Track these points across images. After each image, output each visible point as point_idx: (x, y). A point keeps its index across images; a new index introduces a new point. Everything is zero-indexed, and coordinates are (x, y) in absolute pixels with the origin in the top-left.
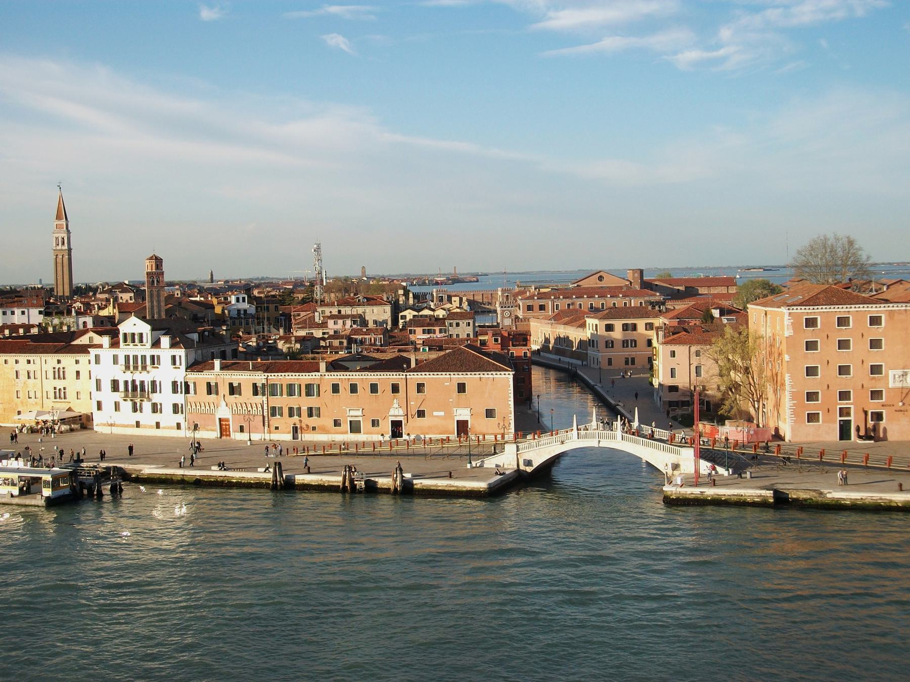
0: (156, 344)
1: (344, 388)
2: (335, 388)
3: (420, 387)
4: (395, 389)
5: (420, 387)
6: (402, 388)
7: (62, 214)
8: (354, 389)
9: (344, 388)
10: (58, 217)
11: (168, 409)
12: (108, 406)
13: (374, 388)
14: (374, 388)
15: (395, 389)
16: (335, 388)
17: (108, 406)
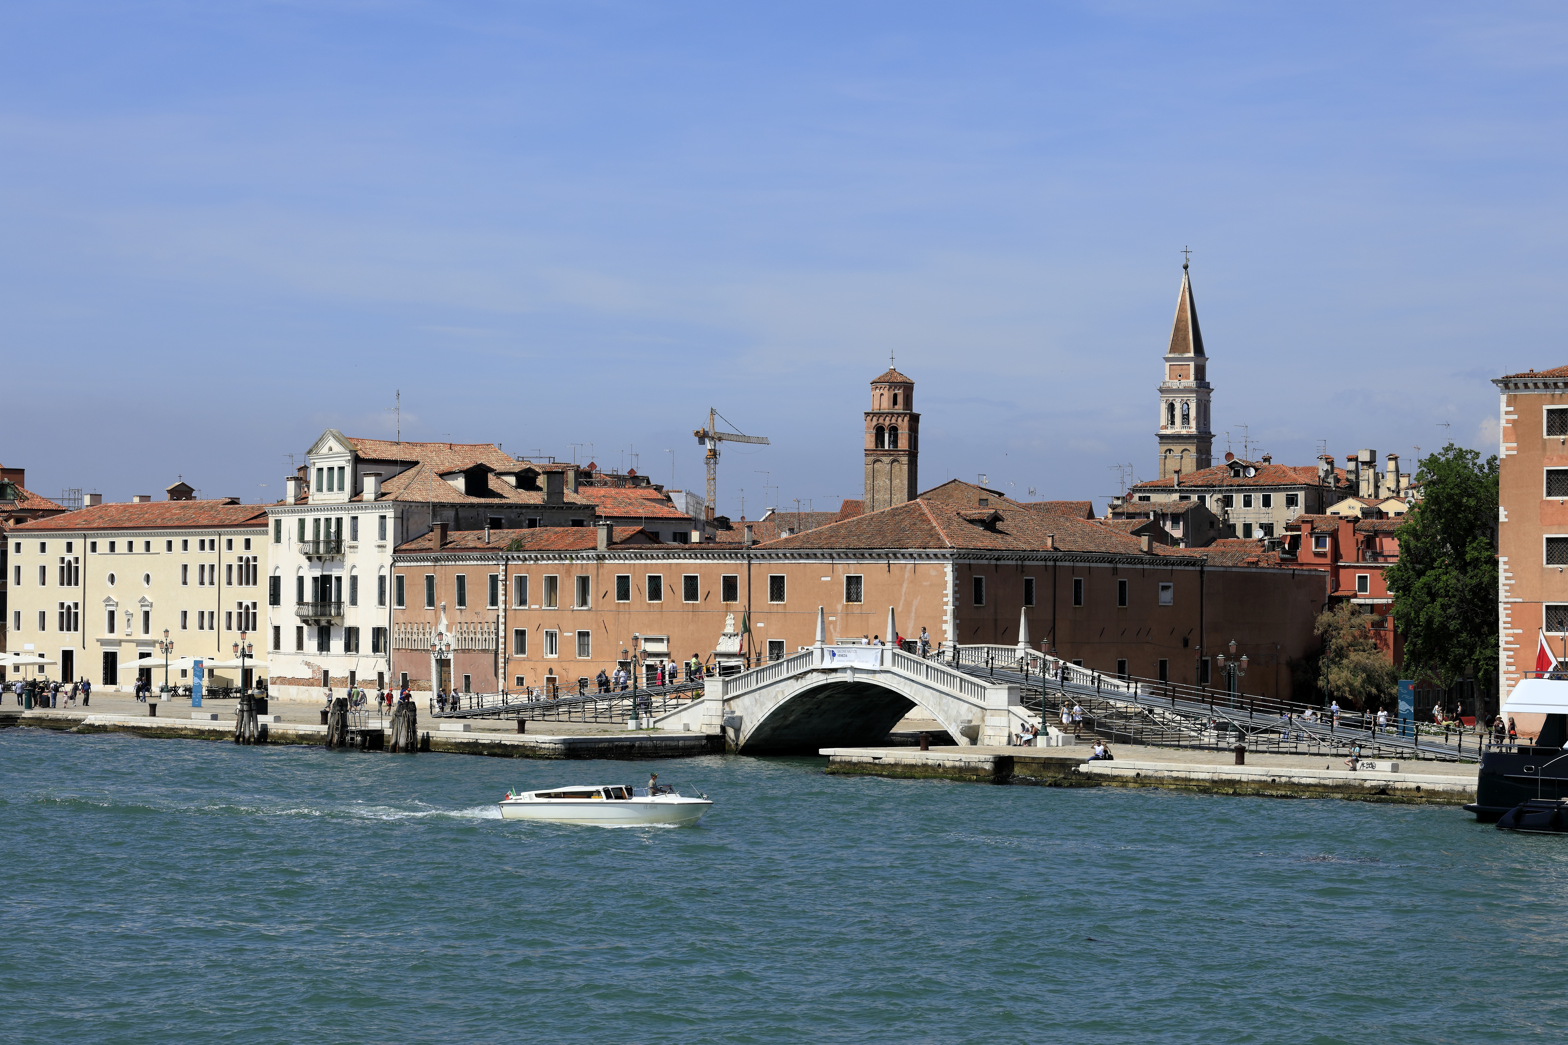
0: (357, 491)
1: (639, 587)
2: (623, 588)
3: (777, 587)
4: (730, 588)
5: (777, 587)
6: (741, 590)
7: (1190, 338)
8: (655, 588)
9: (639, 587)
10: (1177, 345)
11: (366, 640)
12: (288, 639)
13: (691, 587)
14: (691, 587)
15: (730, 588)
16: (623, 588)
17: (288, 639)
